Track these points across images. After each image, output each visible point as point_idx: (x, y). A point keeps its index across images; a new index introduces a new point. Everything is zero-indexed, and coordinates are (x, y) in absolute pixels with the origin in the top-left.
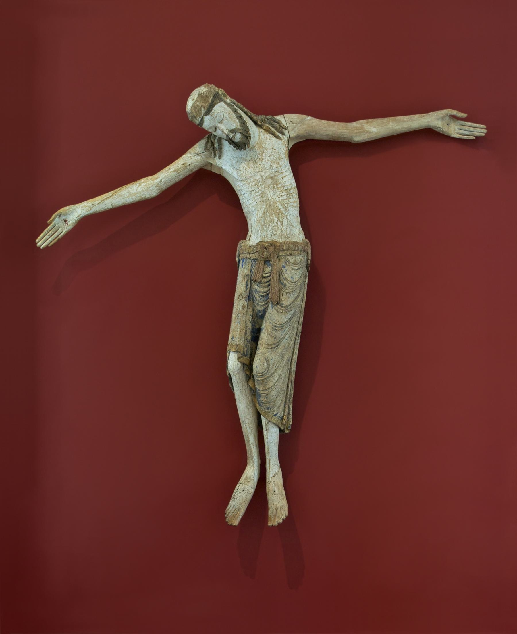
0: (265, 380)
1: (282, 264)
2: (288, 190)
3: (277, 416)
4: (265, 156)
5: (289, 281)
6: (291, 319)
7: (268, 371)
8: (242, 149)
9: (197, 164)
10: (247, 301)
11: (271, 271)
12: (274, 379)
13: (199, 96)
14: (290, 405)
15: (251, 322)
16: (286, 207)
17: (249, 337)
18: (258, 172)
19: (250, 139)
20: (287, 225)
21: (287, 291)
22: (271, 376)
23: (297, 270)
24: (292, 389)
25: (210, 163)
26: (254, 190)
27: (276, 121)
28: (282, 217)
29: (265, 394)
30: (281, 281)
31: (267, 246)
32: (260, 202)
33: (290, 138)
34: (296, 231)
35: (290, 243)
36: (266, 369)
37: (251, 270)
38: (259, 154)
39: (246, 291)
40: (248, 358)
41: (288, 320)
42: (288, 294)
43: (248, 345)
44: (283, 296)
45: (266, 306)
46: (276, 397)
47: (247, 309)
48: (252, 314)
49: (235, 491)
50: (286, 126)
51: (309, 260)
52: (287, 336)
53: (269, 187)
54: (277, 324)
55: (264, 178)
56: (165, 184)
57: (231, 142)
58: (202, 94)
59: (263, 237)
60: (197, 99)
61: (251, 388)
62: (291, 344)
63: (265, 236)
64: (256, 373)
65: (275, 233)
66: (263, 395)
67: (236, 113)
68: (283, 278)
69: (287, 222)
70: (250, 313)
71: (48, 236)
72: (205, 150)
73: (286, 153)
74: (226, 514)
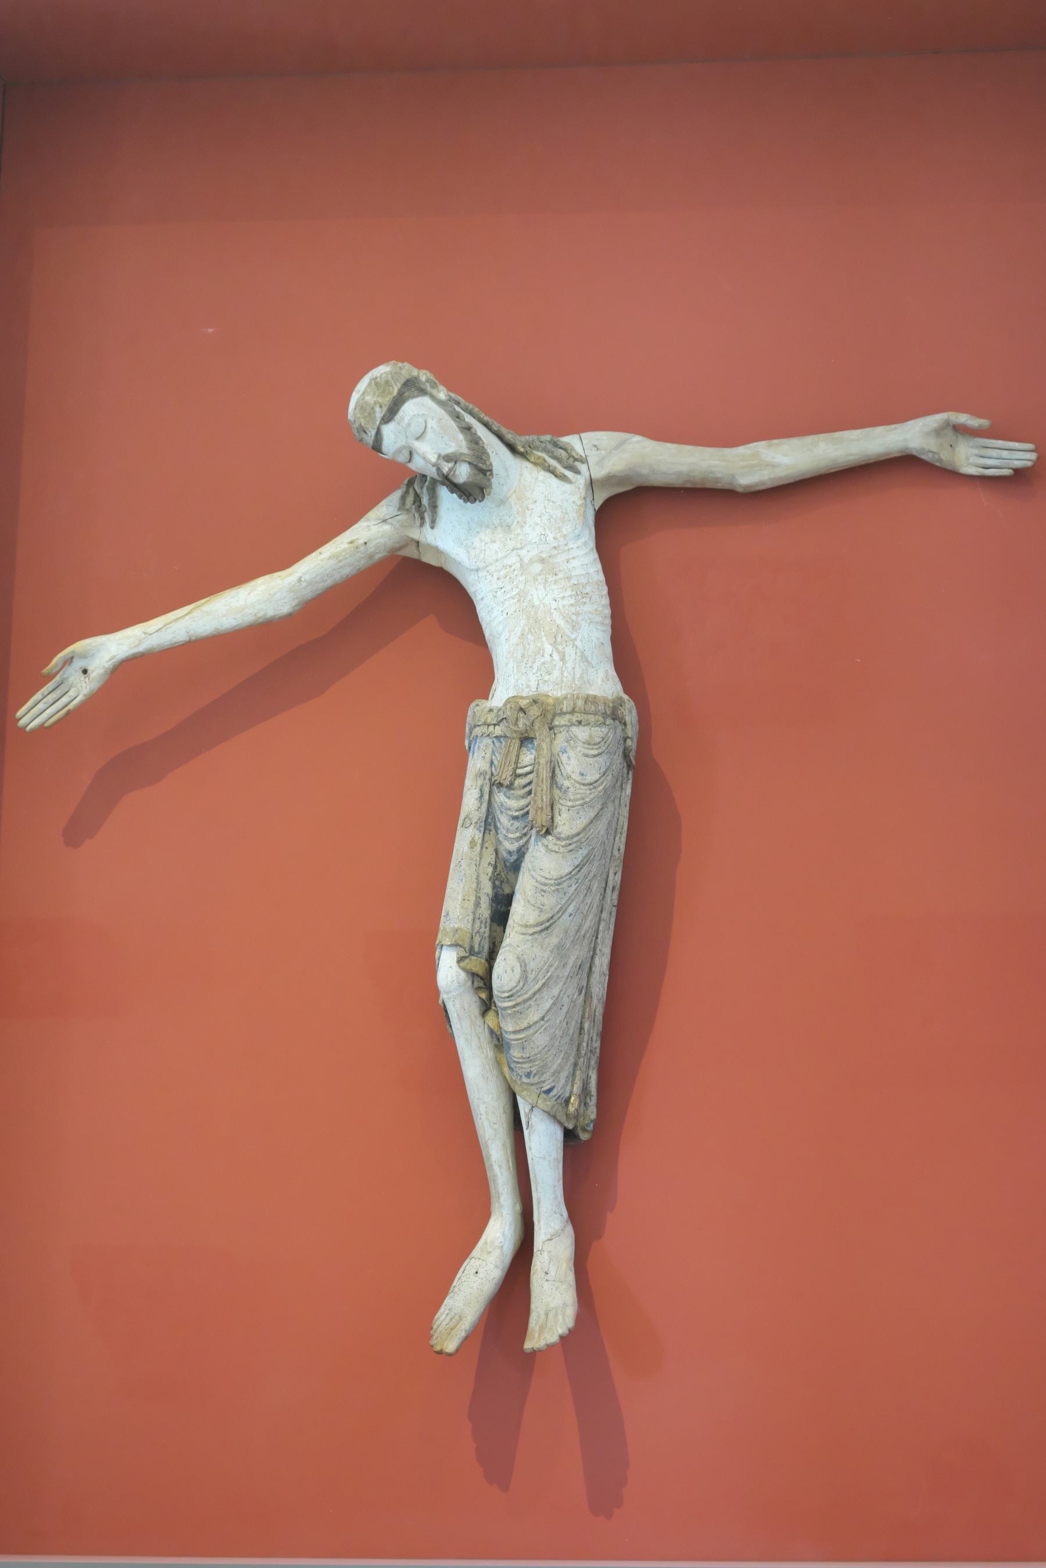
0: (518, 1008)
1: (559, 746)
2: (581, 586)
3: (552, 1094)
4: (531, 515)
5: (575, 780)
6: (581, 869)
7: (524, 985)
8: (475, 501)
9: (382, 540)
10: (480, 831)
11: (535, 760)
12: (540, 1005)
13: (370, 384)
14: (590, 1074)
15: (490, 880)
16: (573, 620)
17: (485, 911)
18: (512, 550)
19: (492, 474)
20: (575, 659)
21: (570, 804)
22: (533, 997)
23: (595, 756)
24: (594, 1039)
25: (413, 540)
26: (501, 588)
27: (560, 444)
28: (564, 642)
29: (520, 1042)
30: (556, 783)
31: (524, 705)
32: (515, 611)
33: (592, 483)
34: (597, 673)
35: (578, 698)
36: (519, 982)
37: (492, 763)
38: (518, 513)
39: (479, 808)
40: (483, 961)
41: (574, 869)
42: (573, 810)
43: (483, 930)
44: (560, 815)
45: (525, 839)
46: (546, 1049)
47: (482, 848)
48: (494, 859)
49: (458, 1276)
50: (584, 456)
51: (628, 740)
52: (571, 909)
53: (537, 580)
54: (547, 879)
55: (526, 560)
56: (310, 587)
57: (456, 488)
58: (378, 379)
59: (519, 688)
60: (366, 388)
61: (492, 1032)
62: (586, 927)
63: (525, 686)
64: (498, 991)
65: (547, 678)
66: (514, 1042)
67: (457, 420)
68: (562, 774)
69: (576, 653)
70: (489, 857)
71: (44, 703)
72: (399, 509)
73: (579, 510)
74: (432, 1328)
